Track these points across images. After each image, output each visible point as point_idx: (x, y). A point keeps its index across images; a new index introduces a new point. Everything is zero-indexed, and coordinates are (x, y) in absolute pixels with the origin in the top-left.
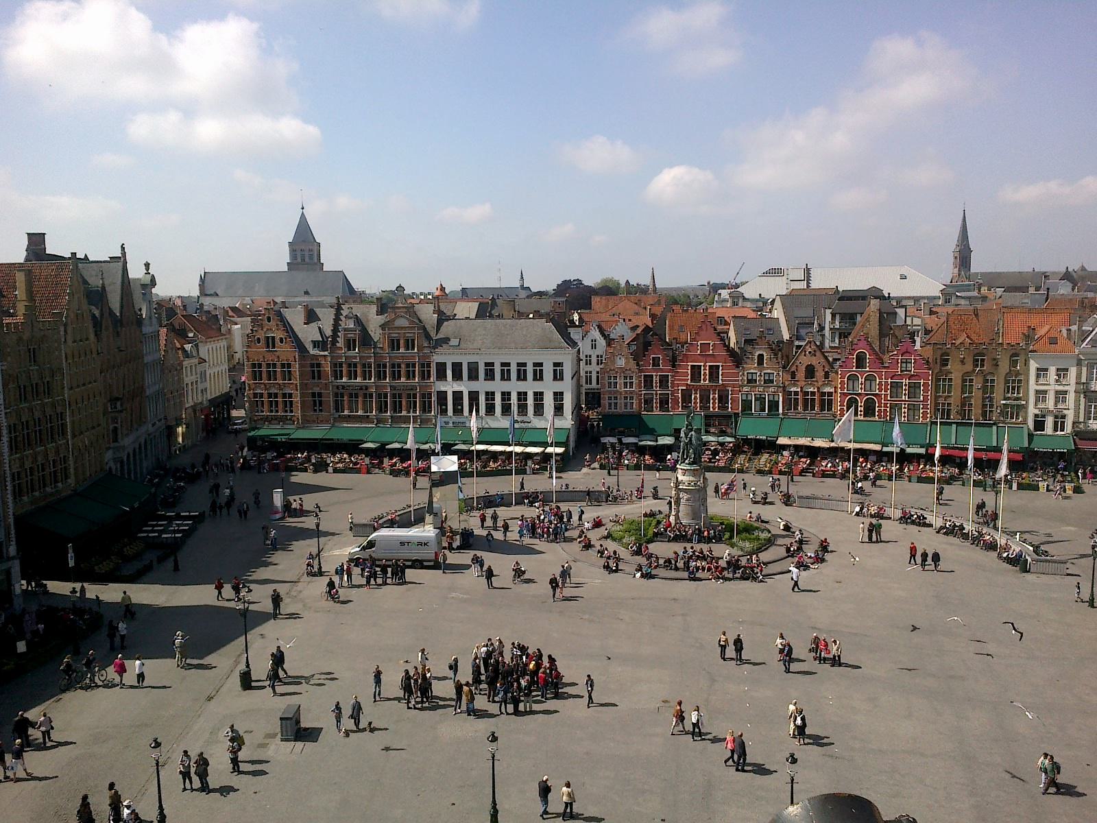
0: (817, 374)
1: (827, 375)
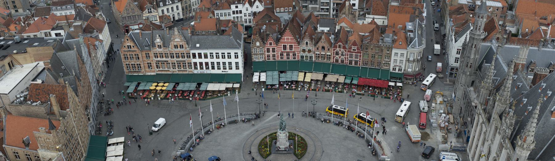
1: (329, 50)
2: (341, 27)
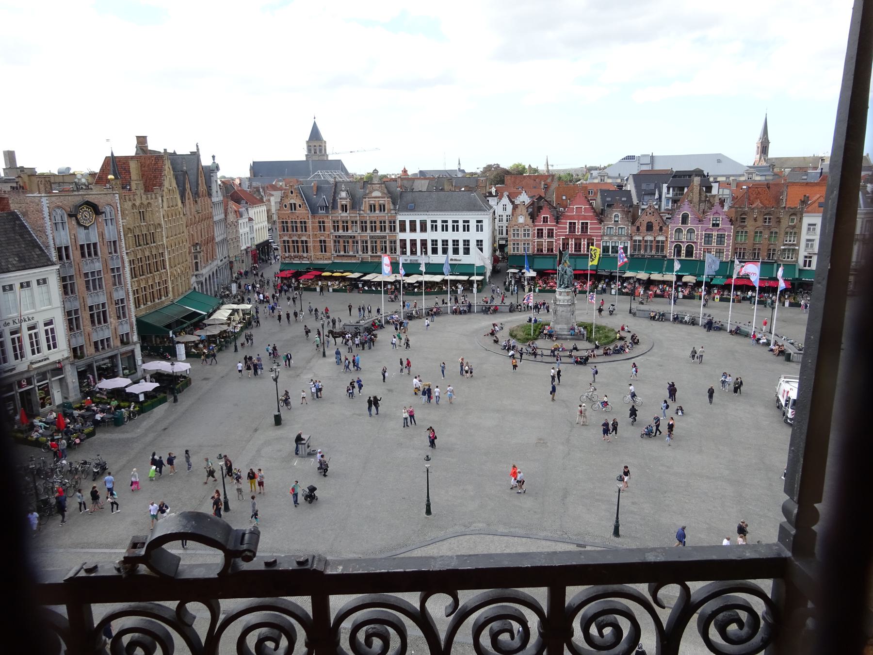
0: (654, 228)
1: (661, 229)
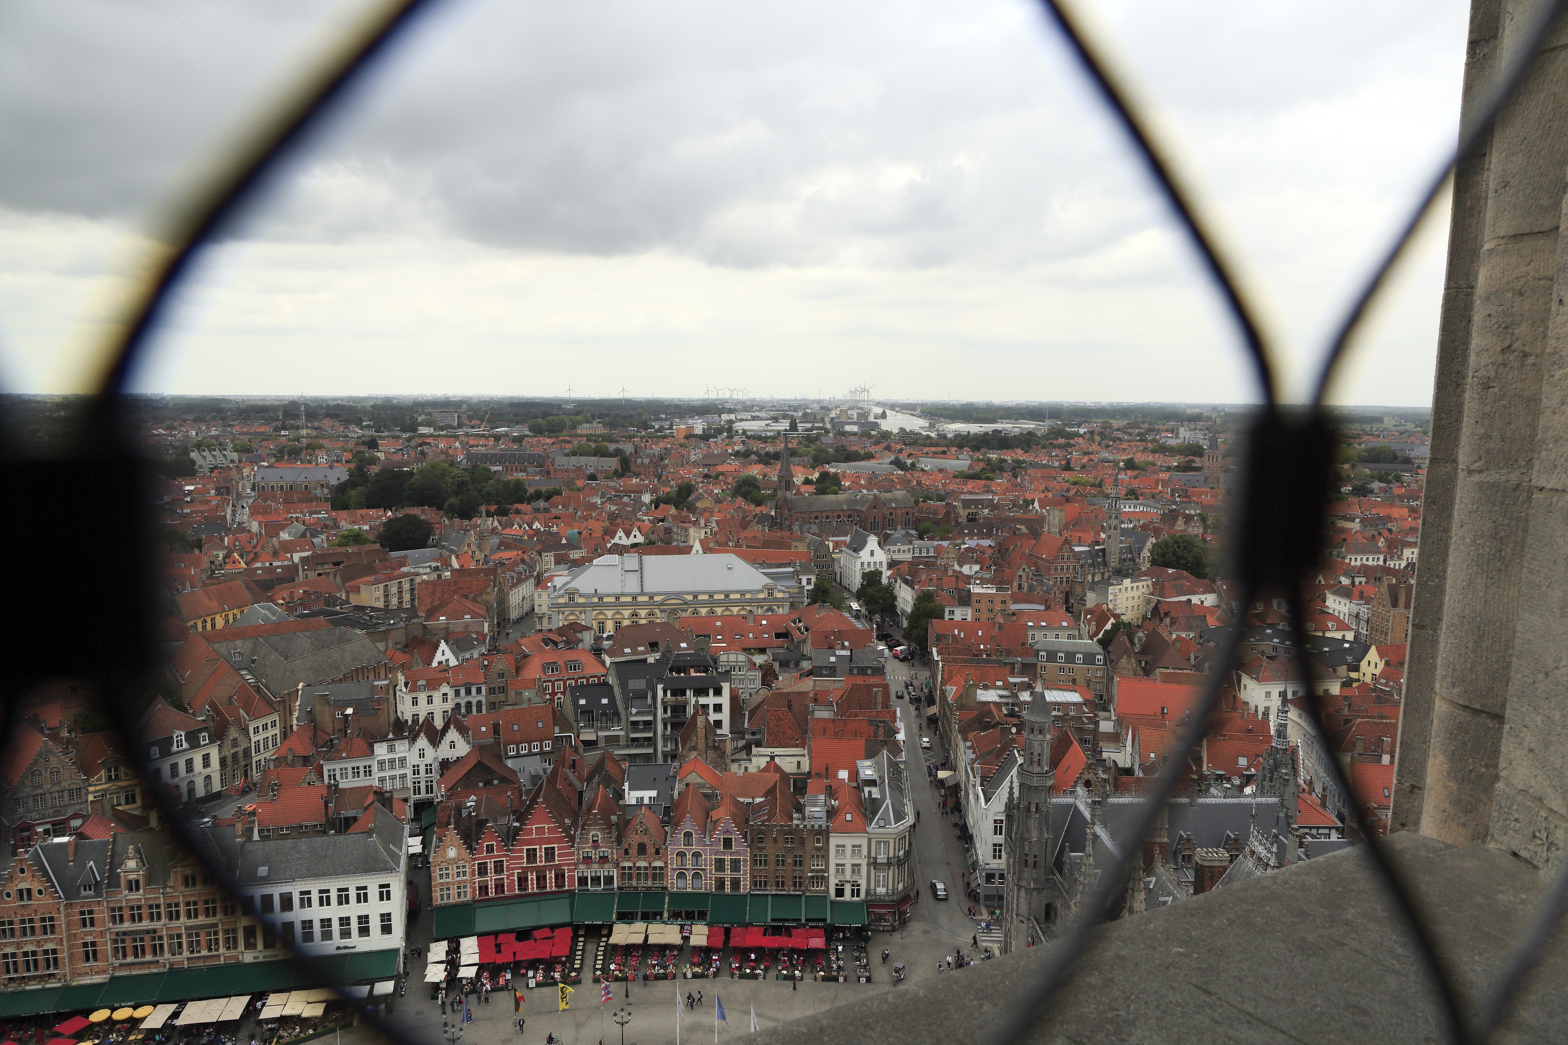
1: (657, 852)
2: (687, 785)
